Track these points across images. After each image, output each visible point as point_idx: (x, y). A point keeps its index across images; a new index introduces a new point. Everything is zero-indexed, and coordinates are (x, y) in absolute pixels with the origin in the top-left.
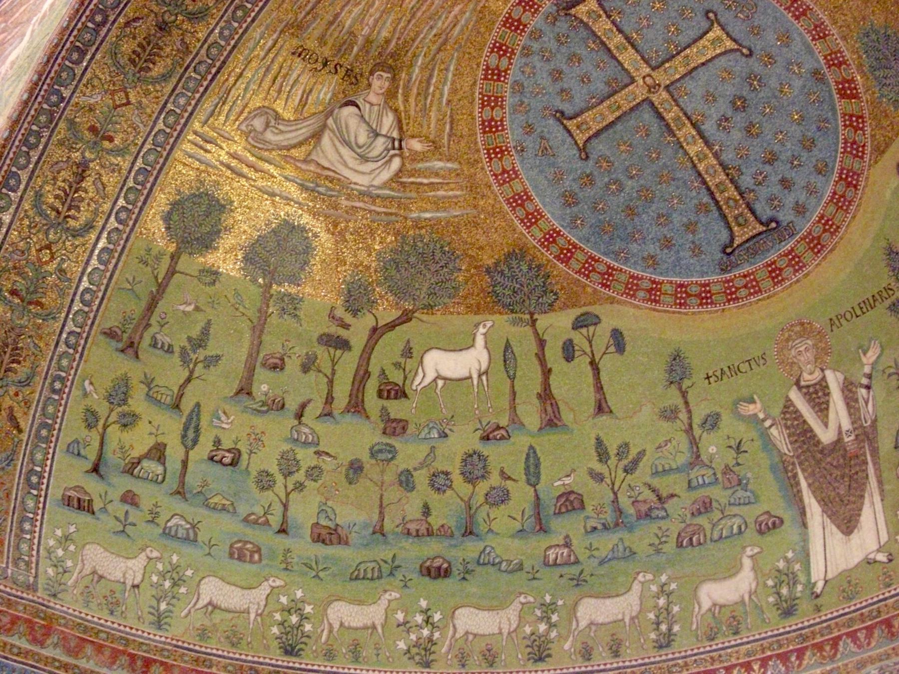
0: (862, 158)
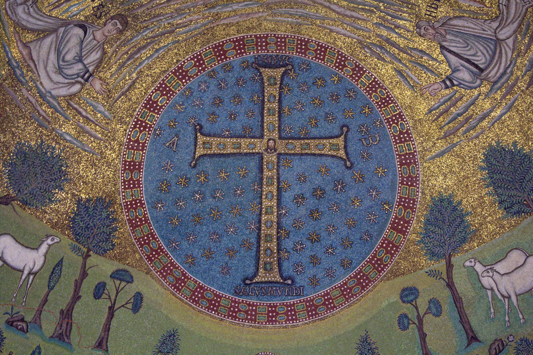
0: (380, 272)
